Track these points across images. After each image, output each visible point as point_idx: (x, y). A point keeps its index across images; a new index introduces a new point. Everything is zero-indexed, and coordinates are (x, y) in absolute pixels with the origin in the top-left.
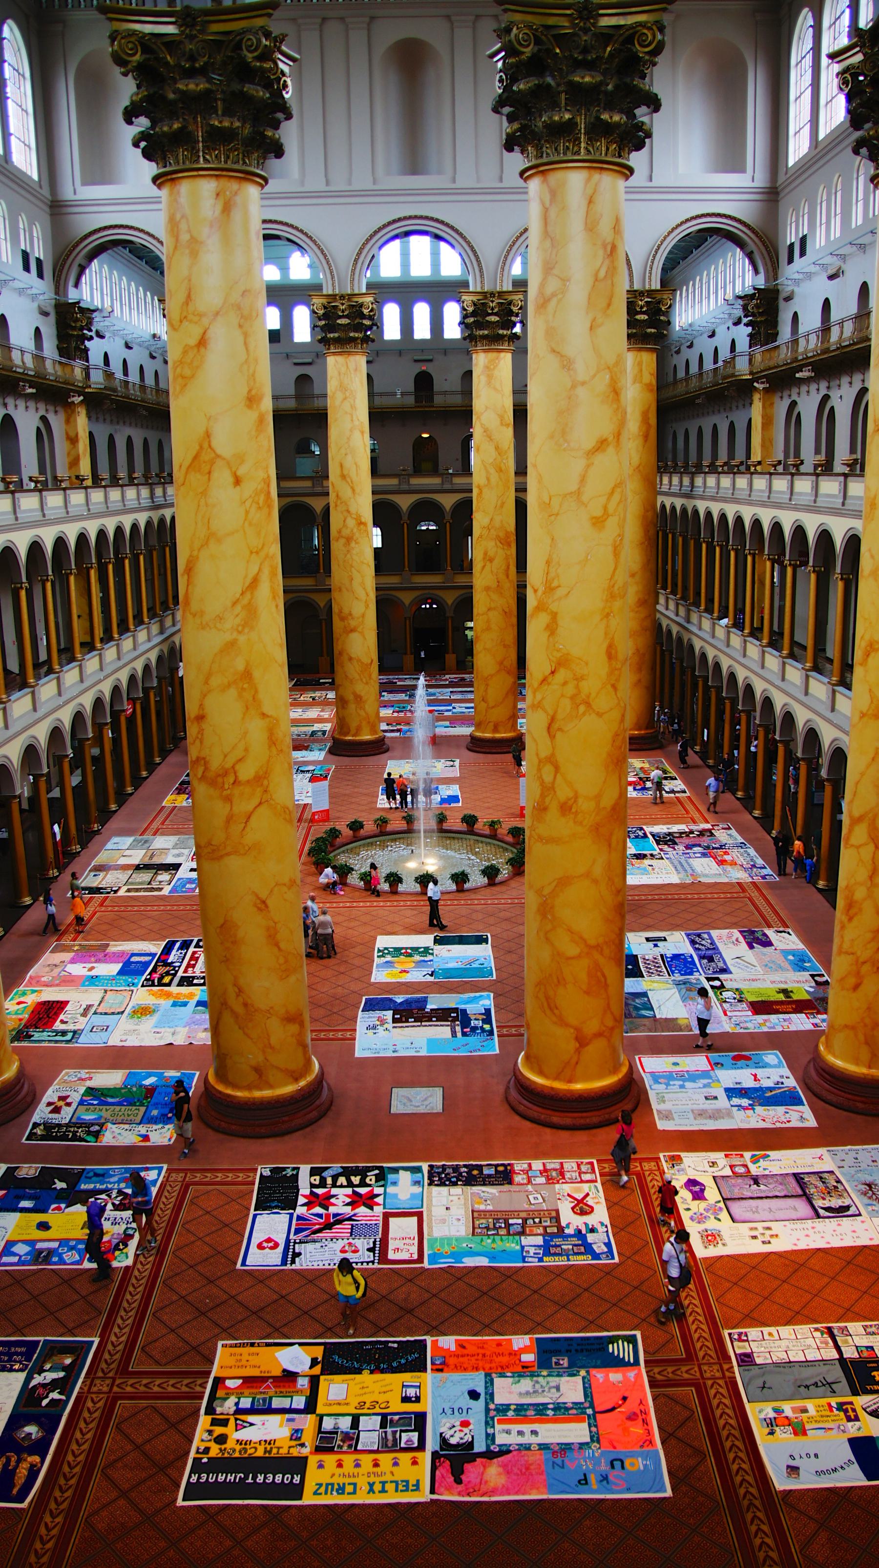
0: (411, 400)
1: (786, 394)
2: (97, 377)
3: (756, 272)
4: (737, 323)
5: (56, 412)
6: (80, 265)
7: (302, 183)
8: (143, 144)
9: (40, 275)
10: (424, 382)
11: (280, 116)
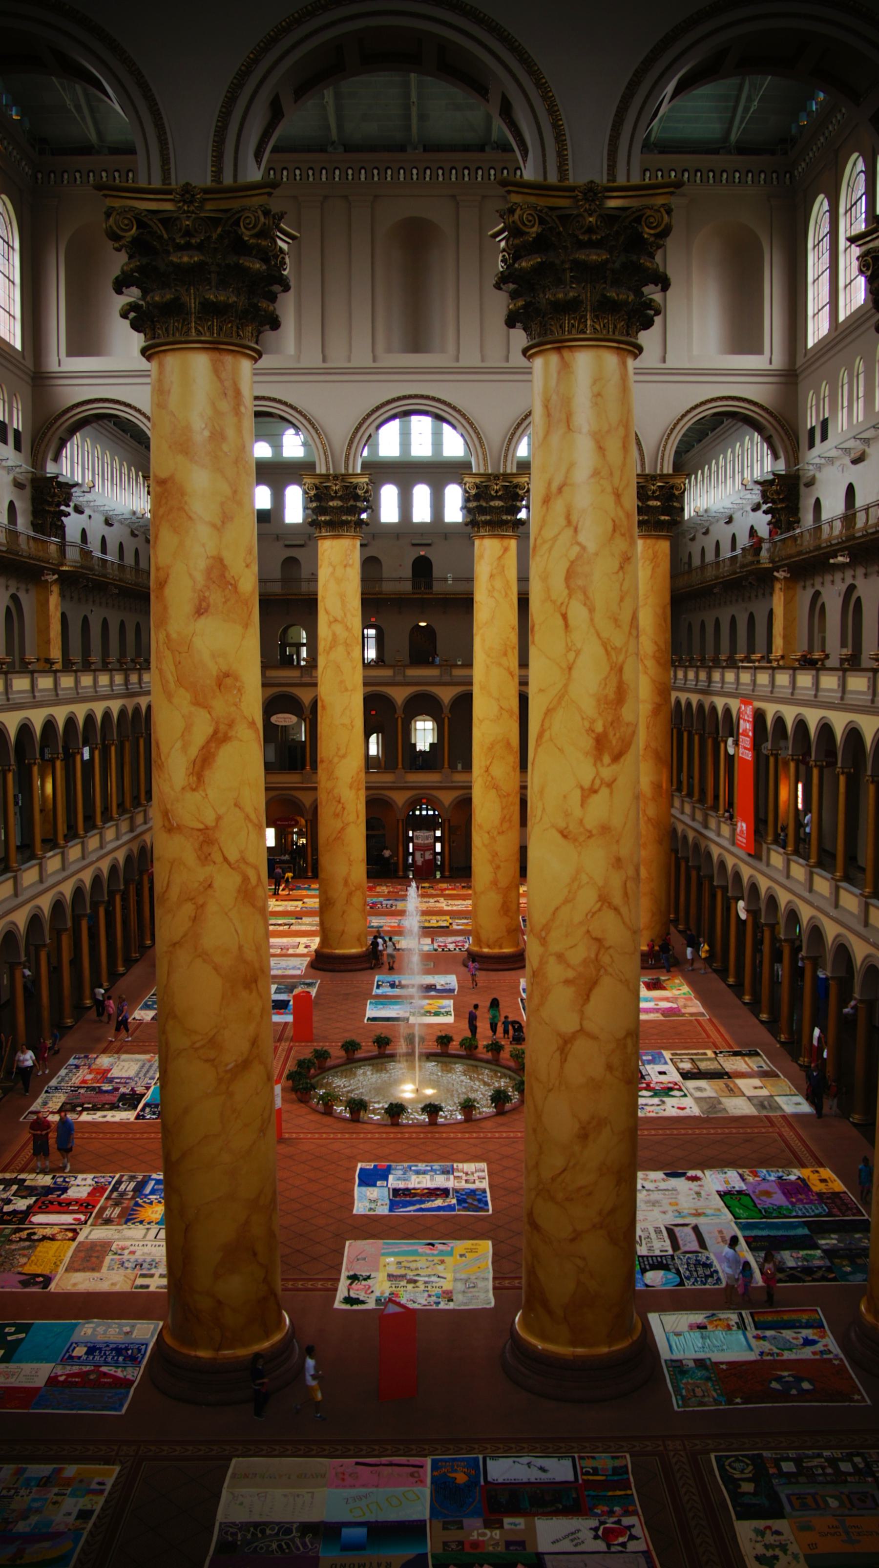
0: (407, 587)
1: (808, 583)
2: (72, 554)
3: (776, 457)
4: (756, 508)
5: (27, 591)
6: (61, 438)
7: (298, 359)
8: (132, 315)
9: (18, 447)
10: (422, 568)
11: (276, 288)
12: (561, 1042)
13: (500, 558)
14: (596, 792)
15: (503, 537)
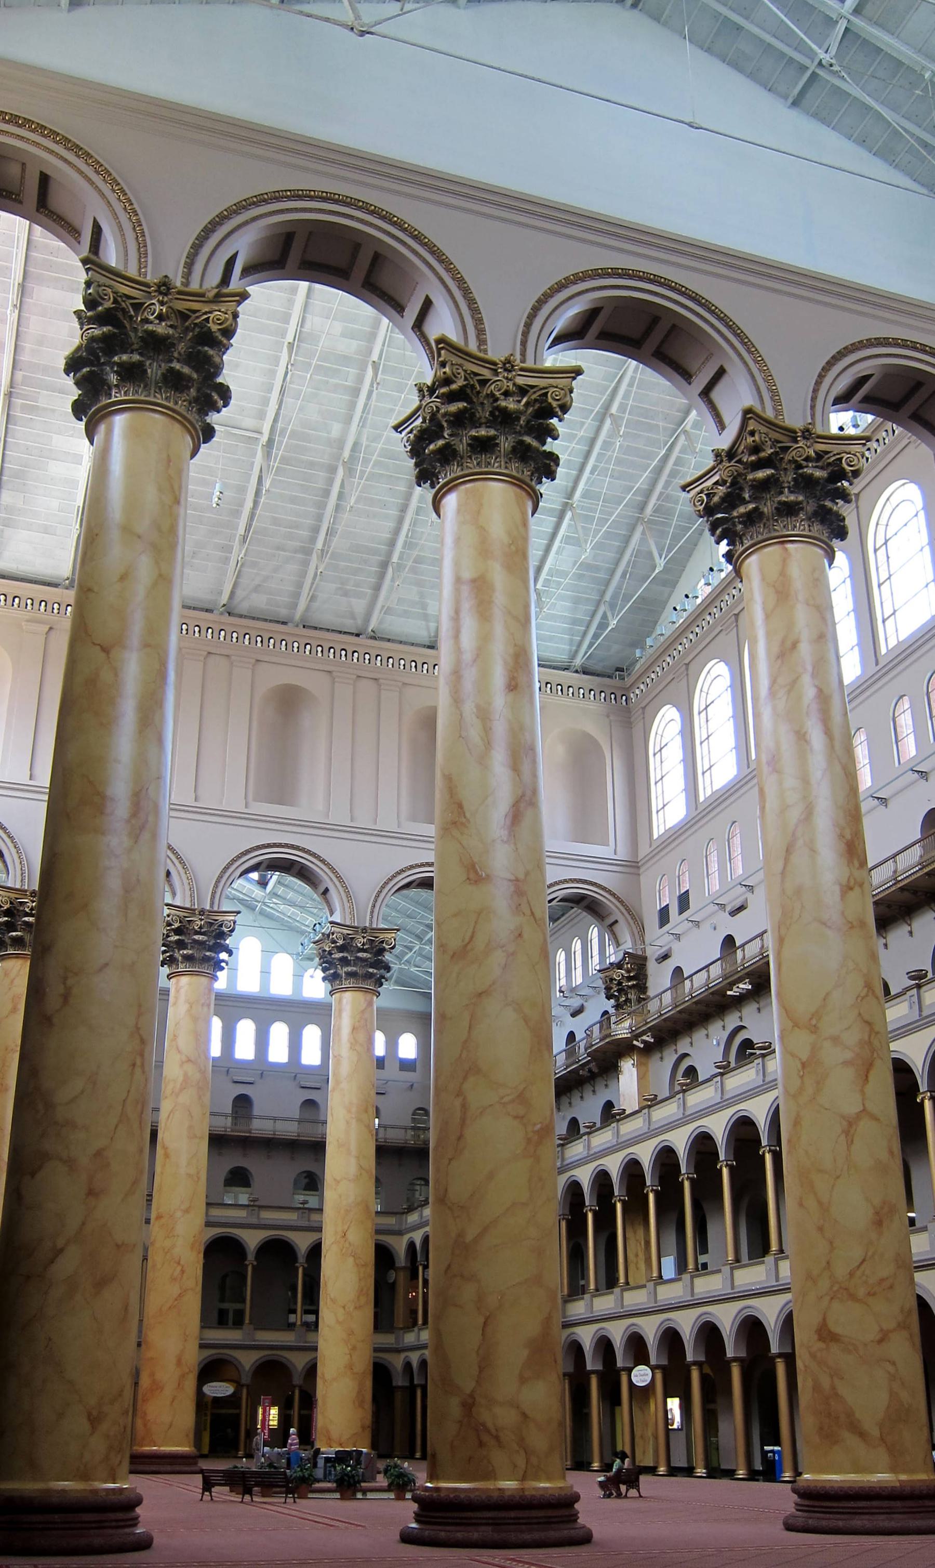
3: (618, 944)
12: (845, 1123)
13: (363, 1012)
14: (851, 889)
15: (367, 990)
